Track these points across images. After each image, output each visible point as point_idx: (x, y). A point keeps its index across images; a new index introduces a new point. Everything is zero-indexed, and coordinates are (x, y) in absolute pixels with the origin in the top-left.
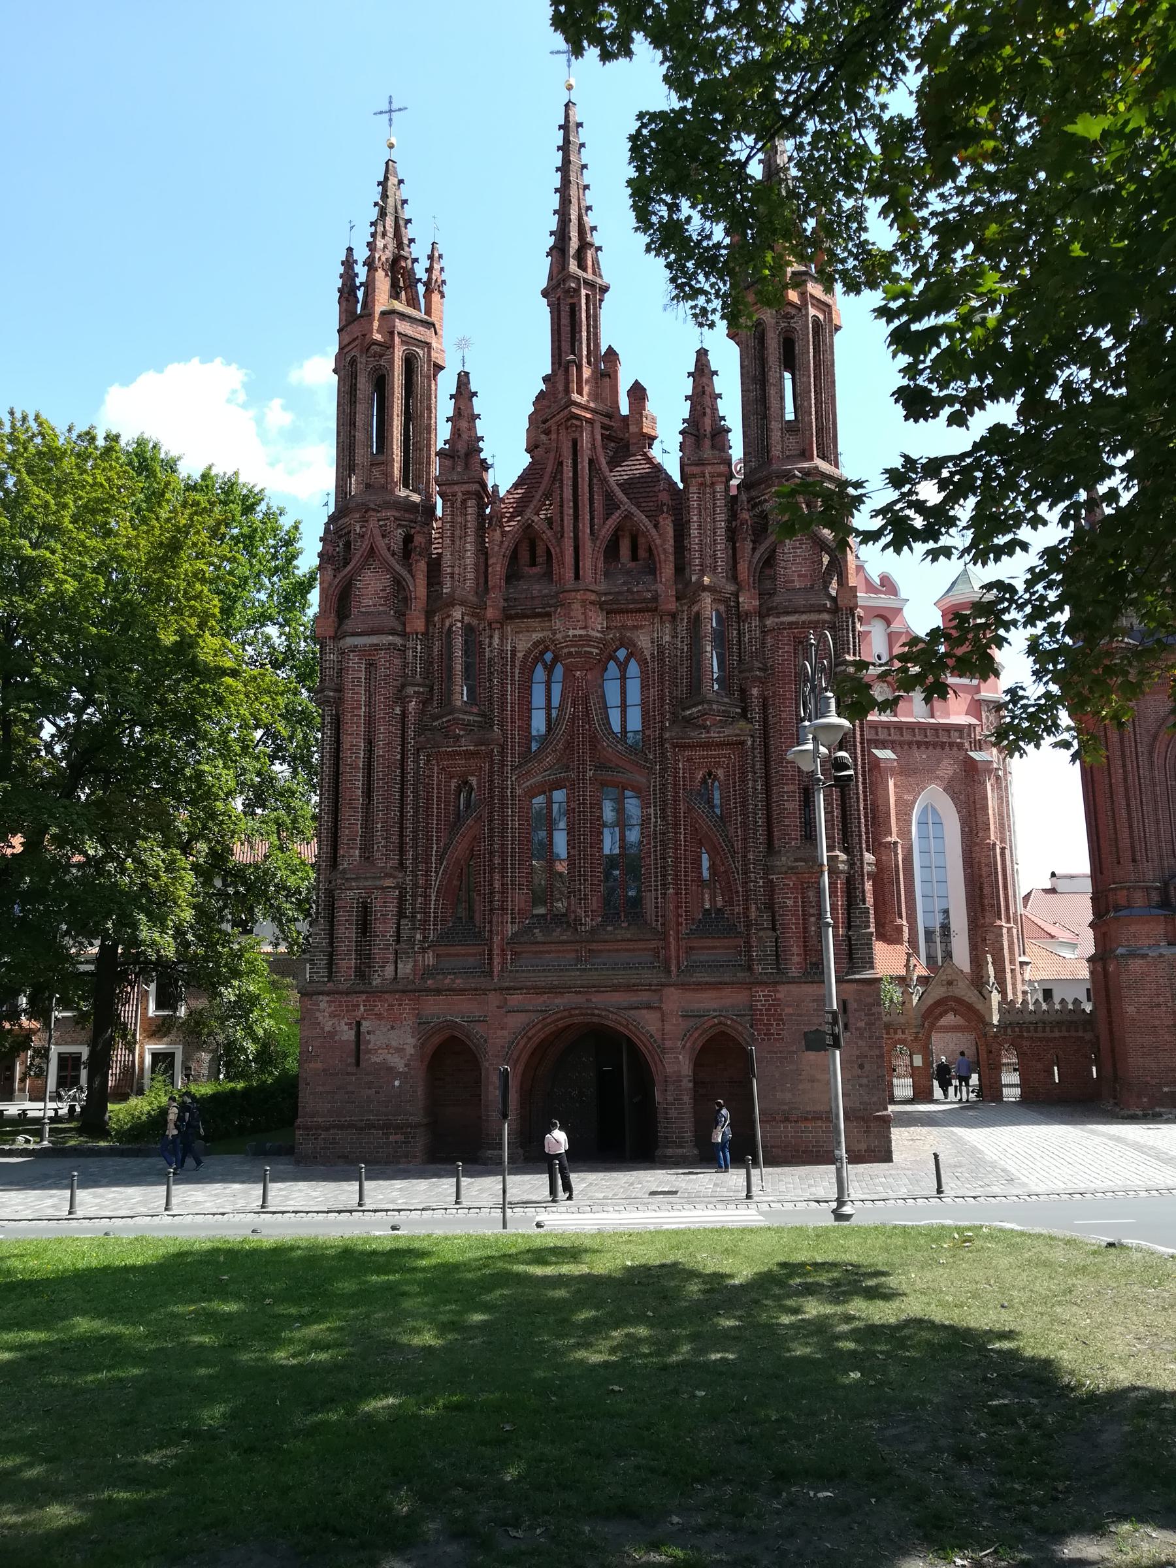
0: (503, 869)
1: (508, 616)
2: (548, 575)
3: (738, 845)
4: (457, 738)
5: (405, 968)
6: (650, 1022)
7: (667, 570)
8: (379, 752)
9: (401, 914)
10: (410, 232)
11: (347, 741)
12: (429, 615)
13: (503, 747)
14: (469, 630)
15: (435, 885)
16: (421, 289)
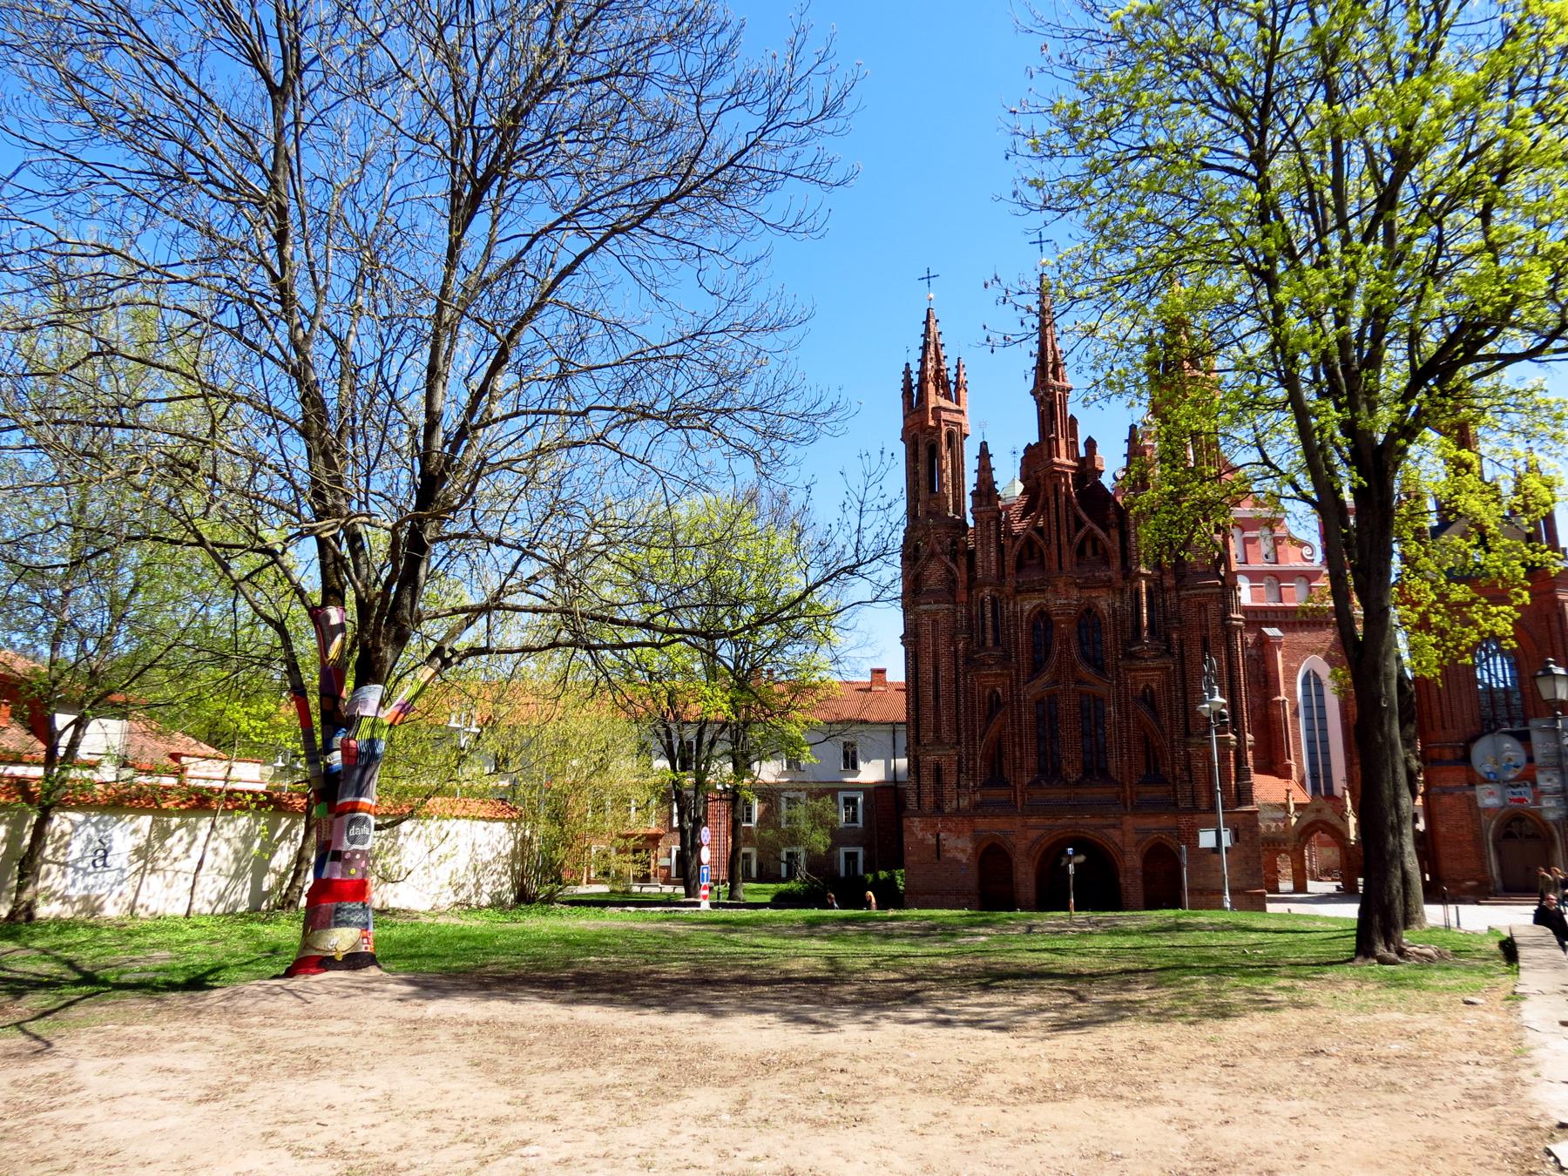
0: (1021, 745)
1: (1018, 591)
2: (1042, 564)
3: (1167, 730)
4: (990, 666)
5: (964, 803)
6: (1115, 835)
7: (1117, 563)
8: (942, 674)
9: (959, 771)
10: (943, 353)
11: (922, 667)
12: (969, 590)
13: (1018, 671)
14: (994, 600)
15: (979, 753)
16: (953, 387)
